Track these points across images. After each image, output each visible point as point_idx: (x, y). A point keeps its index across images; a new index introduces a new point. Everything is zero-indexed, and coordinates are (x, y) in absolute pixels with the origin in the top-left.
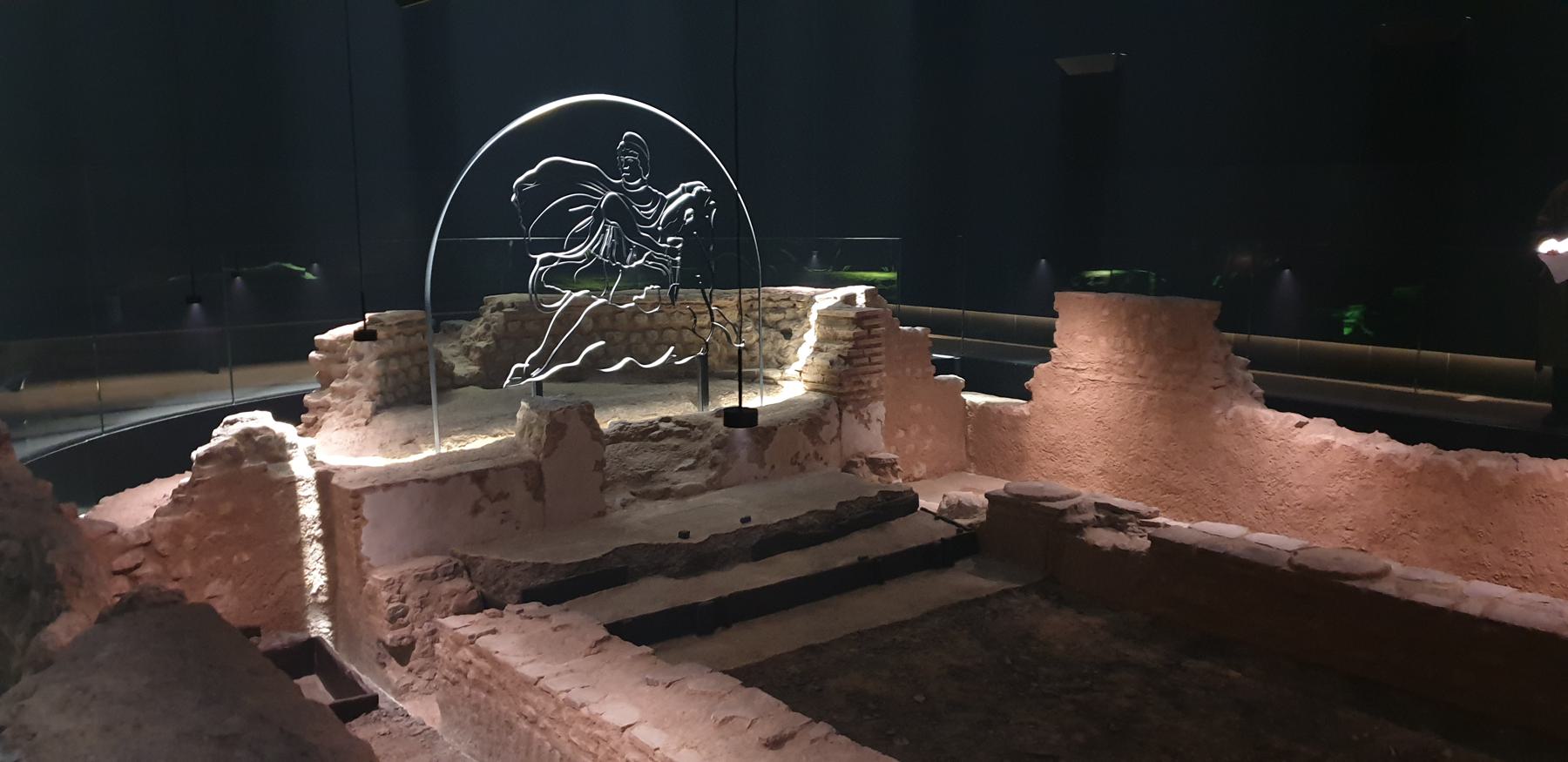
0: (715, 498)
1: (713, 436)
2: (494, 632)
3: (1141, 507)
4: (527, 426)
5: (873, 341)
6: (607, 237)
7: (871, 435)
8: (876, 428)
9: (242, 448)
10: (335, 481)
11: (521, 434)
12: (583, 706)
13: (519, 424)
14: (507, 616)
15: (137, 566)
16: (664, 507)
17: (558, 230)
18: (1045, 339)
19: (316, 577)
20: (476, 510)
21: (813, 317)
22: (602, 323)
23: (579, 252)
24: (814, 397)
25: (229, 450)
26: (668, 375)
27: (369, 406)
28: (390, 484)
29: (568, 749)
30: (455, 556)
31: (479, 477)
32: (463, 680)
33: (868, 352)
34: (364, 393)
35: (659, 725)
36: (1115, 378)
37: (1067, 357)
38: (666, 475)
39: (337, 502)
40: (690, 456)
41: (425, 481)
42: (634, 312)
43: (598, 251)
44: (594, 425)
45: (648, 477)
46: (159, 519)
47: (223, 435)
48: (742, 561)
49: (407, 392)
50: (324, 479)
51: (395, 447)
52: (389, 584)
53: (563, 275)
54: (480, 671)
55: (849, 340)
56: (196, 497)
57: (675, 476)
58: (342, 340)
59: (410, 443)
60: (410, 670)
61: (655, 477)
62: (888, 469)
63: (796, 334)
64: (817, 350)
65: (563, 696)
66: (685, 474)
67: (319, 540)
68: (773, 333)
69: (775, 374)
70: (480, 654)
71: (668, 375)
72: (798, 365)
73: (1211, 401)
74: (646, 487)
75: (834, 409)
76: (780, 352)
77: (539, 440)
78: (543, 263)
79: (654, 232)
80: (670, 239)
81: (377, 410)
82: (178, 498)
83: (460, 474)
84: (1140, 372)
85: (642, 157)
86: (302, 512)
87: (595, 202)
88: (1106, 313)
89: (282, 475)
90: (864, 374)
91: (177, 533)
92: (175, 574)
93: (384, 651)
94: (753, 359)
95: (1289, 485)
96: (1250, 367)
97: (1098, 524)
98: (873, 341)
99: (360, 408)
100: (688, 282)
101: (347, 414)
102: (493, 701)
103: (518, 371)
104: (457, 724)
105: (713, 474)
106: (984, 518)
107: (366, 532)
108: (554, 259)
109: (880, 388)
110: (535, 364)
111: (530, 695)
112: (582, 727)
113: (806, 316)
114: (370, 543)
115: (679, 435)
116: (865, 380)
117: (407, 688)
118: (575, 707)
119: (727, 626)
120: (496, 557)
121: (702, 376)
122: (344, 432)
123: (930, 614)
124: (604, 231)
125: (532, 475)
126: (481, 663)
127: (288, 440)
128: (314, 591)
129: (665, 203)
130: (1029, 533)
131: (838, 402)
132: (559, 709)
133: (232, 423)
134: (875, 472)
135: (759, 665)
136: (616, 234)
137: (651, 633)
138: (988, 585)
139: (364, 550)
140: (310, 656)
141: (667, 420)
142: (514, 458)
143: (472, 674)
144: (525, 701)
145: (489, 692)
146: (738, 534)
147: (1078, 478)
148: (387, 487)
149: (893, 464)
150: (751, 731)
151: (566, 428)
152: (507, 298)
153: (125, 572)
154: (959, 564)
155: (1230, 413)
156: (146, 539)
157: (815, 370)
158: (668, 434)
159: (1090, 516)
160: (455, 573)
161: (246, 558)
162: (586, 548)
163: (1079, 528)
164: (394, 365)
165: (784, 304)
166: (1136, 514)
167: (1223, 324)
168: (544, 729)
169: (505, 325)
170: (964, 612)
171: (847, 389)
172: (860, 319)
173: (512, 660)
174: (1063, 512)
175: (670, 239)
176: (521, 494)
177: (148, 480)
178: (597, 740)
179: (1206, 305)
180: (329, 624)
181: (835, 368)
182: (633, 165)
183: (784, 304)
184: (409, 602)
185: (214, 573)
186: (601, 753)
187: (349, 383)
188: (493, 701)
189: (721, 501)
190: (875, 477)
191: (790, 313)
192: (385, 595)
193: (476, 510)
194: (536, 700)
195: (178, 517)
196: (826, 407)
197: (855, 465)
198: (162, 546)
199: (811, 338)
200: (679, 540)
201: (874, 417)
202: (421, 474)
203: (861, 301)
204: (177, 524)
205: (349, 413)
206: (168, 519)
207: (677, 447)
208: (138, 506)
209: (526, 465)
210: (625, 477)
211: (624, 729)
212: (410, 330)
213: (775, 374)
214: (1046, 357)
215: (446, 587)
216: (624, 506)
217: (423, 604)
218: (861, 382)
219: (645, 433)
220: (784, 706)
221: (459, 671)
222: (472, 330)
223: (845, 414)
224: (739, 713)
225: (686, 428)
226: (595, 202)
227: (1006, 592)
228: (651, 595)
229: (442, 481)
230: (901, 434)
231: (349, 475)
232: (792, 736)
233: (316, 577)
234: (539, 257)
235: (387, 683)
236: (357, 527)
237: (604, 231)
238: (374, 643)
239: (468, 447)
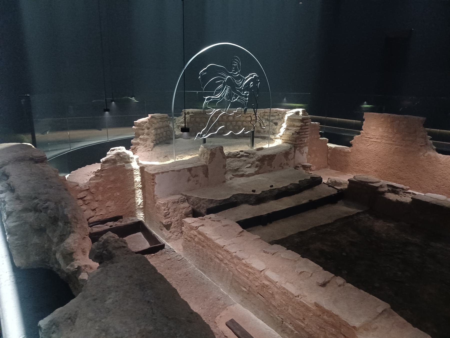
0: (257, 177)
1: (256, 157)
2: (203, 225)
3: (405, 187)
4: (203, 153)
5: (306, 127)
6: (226, 91)
7: (303, 158)
8: (305, 155)
9: (117, 159)
10: (145, 170)
11: (201, 155)
12: (243, 259)
13: (200, 152)
14: (206, 220)
15: (85, 197)
16: (242, 180)
17: (212, 89)
18: (359, 127)
19: (139, 200)
20: (189, 180)
21: (286, 118)
22: (224, 120)
23: (218, 96)
24: (285, 145)
25: (113, 160)
26: (243, 136)
27: (152, 144)
28: (164, 171)
29: (236, 272)
30: (183, 195)
31: (190, 170)
32: (193, 241)
33: (305, 130)
34: (150, 140)
35: (274, 270)
36: (384, 141)
37: (367, 134)
38: (242, 169)
39: (146, 177)
40: (249, 163)
41: (174, 171)
42: (234, 116)
43: (224, 96)
44: (222, 152)
45: (237, 170)
46: (91, 182)
47: (110, 154)
48: (273, 200)
49: (163, 139)
50: (142, 169)
51: (162, 158)
52: (164, 204)
53: (213, 103)
54: (200, 239)
55: (299, 127)
56: (103, 175)
57: (245, 170)
58: (142, 122)
59: (166, 157)
60: (170, 232)
61: (239, 170)
62: (308, 169)
63: (279, 124)
64: (287, 129)
65: (234, 254)
66: (248, 169)
67: (140, 188)
68: (271, 123)
69: (272, 137)
70: (200, 233)
71: (243, 136)
72: (281, 134)
73: (419, 150)
74: (237, 173)
75: (293, 149)
76: (273, 129)
77: (207, 158)
78: (208, 99)
79: (240, 90)
80: (245, 92)
81: (155, 146)
82: (98, 174)
83: (184, 169)
84: (393, 140)
85: (238, 64)
86: (135, 180)
87: (223, 80)
88: (382, 120)
89: (129, 168)
90: (304, 138)
91: (97, 186)
92: (96, 199)
93: (162, 225)
94: (264, 132)
95: (447, 179)
96: (431, 139)
97: (389, 191)
98: (306, 127)
99: (149, 145)
100: (249, 106)
101: (145, 147)
102: (205, 250)
103: (199, 135)
104: (190, 254)
105: (257, 169)
106: (346, 187)
107: (156, 186)
108: (211, 98)
109: (307, 143)
110: (204, 133)
111: (220, 251)
112: (243, 267)
113: (282, 118)
114: (157, 190)
115: (246, 156)
116: (303, 139)
117: (170, 238)
118: (239, 259)
119: (271, 222)
120: (196, 196)
122: (145, 152)
123: (336, 221)
124: (226, 89)
125: (205, 169)
126: (200, 236)
127: (131, 156)
128: (139, 204)
129: (245, 80)
130: (361, 193)
131: (294, 147)
132: (233, 258)
133: (113, 150)
134: (304, 169)
135: (286, 238)
136: (230, 90)
137: (247, 225)
138: (352, 210)
139: (155, 193)
140: (138, 227)
141: (242, 151)
142: (199, 164)
143: (196, 239)
144: (218, 253)
145: (203, 246)
146: (270, 191)
147: (367, 172)
148: (163, 173)
149: (310, 167)
150: (311, 278)
151: (216, 154)
152: (190, 110)
153: (81, 199)
154: (338, 202)
155: (426, 155)
156: (87, 188)
157: (287, 136)
158: (242, 156)
159: (386, 189)
160: (184, 201)
161: (118, 194)
162: (222, 195)
163: (383, 193)
164: (159, 131)
165: (275, 114)
166: (403, 189)
167: (426, 125)
168: (226, 264)
169: (190, 119)
170: (347, 221)
171: (298, 143)
172: (303, 120)
173: (213, 238)
174: (377, 187)
175: (245, 92)
176: (201, 175)
177: (84, 165)
178: (249, 273)
179: (422, 118)
180: (143, 215)
181: (294, 136)
182: (236, 67)
183: (275, 114)
184: (170, 210)
185: (109, 199)
186: (251, 277)
187: (146, 137)
188: (205, 250)
189: (260, 178)
190: (304, 171)
191: (277, 117)
192: (163, 208)
193: (189, 180)
194: (223, 253)
195: (98, 181)
196: (291, 149)
197: (298, 167)
198: (92, 190)
199: (284, 125)
200: (252, 193)
201: (305, 152)
202: (172, 168)
203: (301, 114)
204: (97, 183)
205: (146, 147)
206: (94, 181)
207: (245, 160)
208: (85, 175)
209: (203, 166)
210: (230, 170)
211: (261, 271)
212: (164, 120)
213: (272, 137)
214: (359, 134)
215: (182, 205)
216: (231, 179)
217: (175, 211)
218: (301, 141)
219: (235, 156)
220: (321, 268)
221: (191, 238)
222: (179, 120)
223: (296, 151)
224: (305, 269)
226: (223, 80)
227: (358, 213)
228: (246, 211)
229: (179, 171)
231: (150, 168)
232: (329, 282)
233: (139, 200)
234: (206, 98)
235: (163, 236)
236: (153, 185)
237: (226, 89)
238: (159, 222)
239: (184, 159)
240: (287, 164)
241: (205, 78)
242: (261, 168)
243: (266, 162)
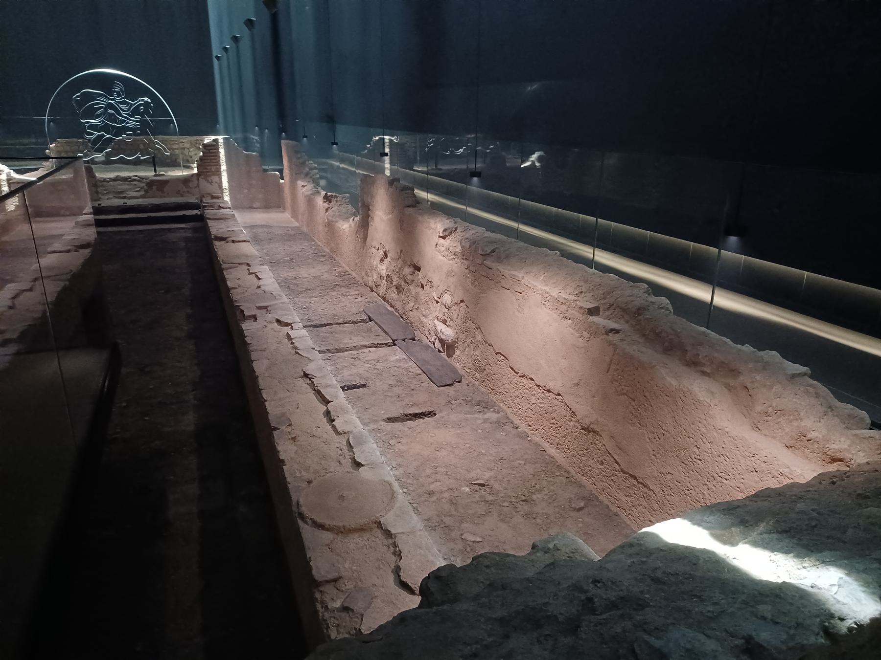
45: (121, 192)
121: (154, 162)
158: (135, 180)
182: (118, 93)
219: (125, 179)
225: (141, 179)
240: (188, 192)
242: (146, 191)
243: (154, 187)
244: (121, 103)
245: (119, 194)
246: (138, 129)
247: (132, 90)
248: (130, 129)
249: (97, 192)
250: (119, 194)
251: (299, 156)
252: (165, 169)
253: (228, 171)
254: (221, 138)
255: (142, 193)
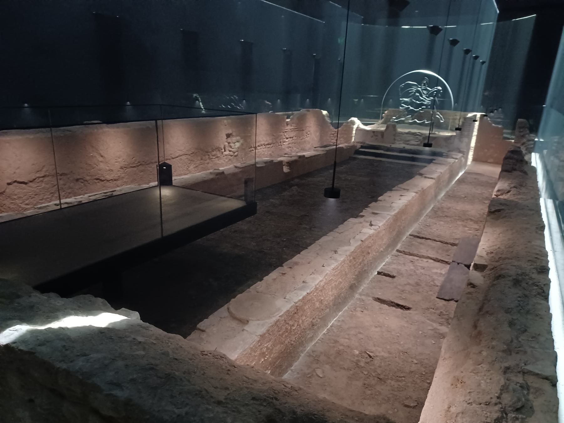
17: (407, 95)
45: (408, 141)
125: (382, 133)
158: (418, 135)
176: (380, 136)
193: (372, 137)
230: (486, 150)
241: (403, 89)
244: (424, 90)
245: (407, 142)
246: (429, 105)
247: (433, 82)
248: (423, 105)
249: (395, 139)
250: (407, 142)
251: (522, 130)
252: (439, 130)
253: (478, 136)
254: (479, 115)
255: (419, 143)
